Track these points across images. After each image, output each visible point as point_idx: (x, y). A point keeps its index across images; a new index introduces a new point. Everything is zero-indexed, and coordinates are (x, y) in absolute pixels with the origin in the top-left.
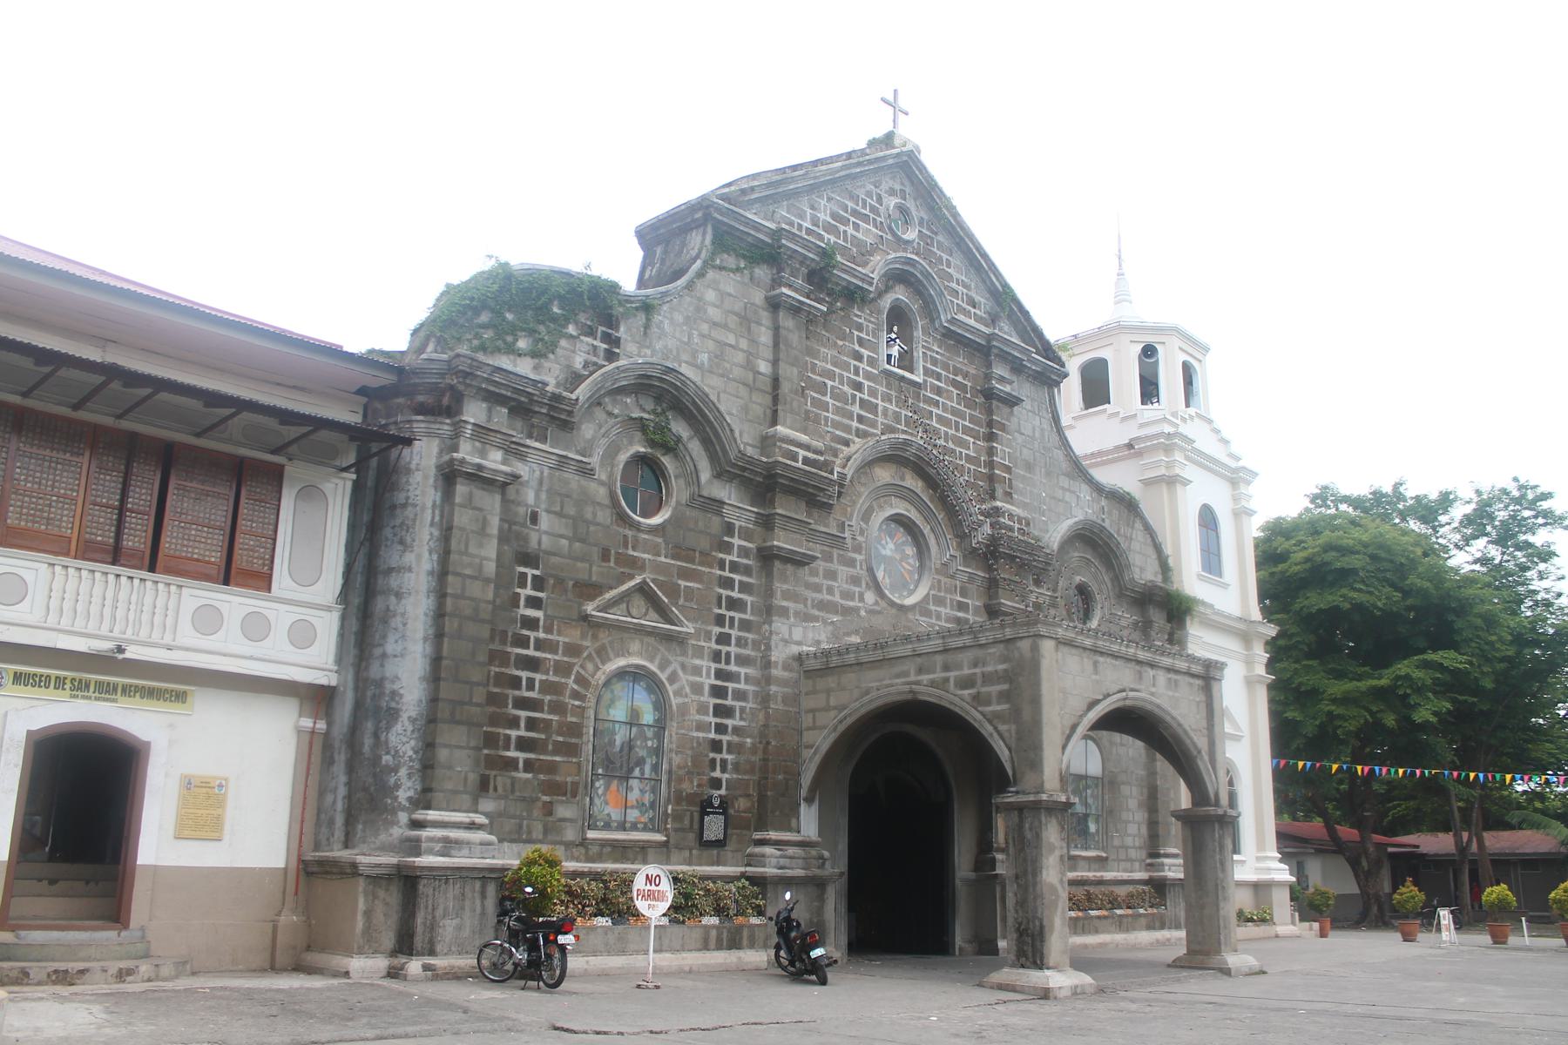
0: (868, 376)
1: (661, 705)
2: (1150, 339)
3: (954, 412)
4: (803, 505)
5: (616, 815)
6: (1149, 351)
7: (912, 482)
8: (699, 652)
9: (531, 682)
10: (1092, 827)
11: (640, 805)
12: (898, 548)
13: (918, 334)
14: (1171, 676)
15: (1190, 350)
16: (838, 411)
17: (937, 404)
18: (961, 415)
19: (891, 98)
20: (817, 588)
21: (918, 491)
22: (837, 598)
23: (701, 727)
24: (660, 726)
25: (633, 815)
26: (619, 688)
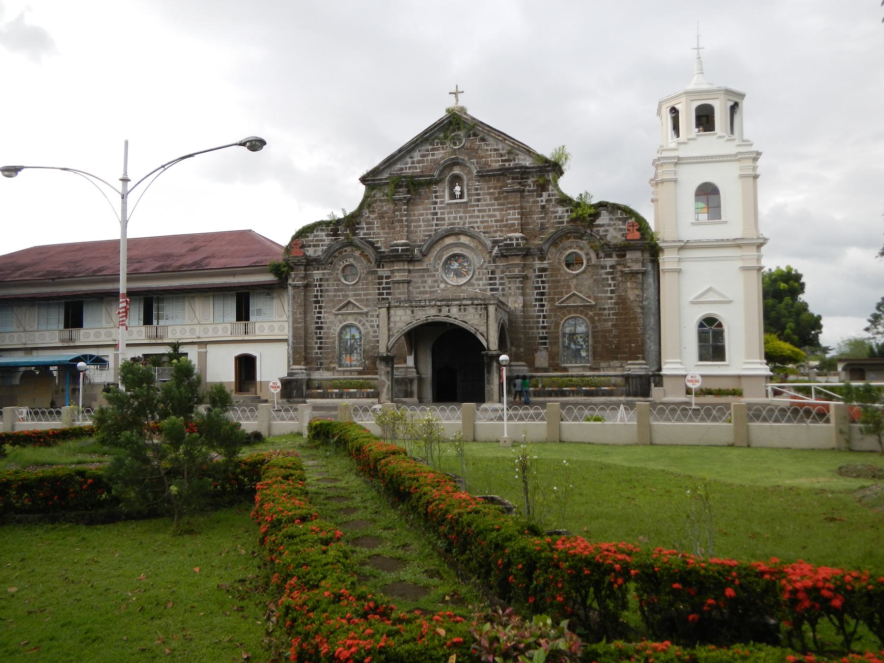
0: (440, 208)
1: (360, 333)
2: (671, 104)
3: (487, 205)
4: (406, 263)
5: (348, 362)
6: (674, 111)
7: (464, 239)
8: (372, 316)
9: (320, 333)
10: (583, 354)
11: (357, 360)
12: (460, 264)
13: (465, 182)
14: (462, 307)
15: (697, 98)
16: (426, 226)
17: (478, 206)
18: (493, 205)
19: (454, 90)
20: (419, 287)
21: (467, 243)
22: (427, 289)
23: (374, 337)
24: (361, 338)
25: (355, 363)
26: (348, 330)
